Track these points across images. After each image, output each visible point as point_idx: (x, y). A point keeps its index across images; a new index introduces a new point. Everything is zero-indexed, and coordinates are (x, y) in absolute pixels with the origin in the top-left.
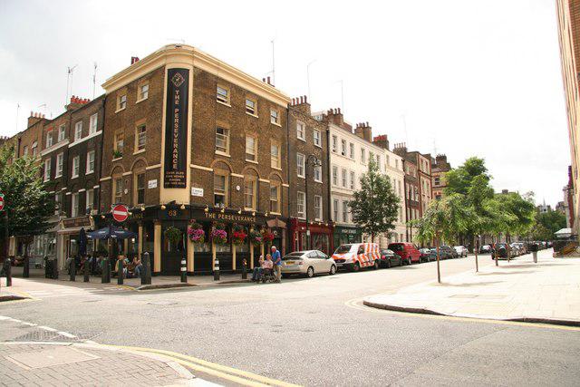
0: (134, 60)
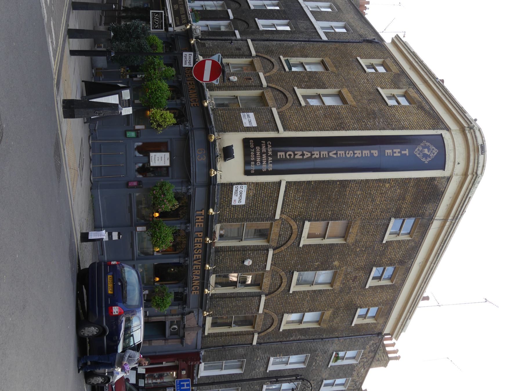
0: (443, 81)
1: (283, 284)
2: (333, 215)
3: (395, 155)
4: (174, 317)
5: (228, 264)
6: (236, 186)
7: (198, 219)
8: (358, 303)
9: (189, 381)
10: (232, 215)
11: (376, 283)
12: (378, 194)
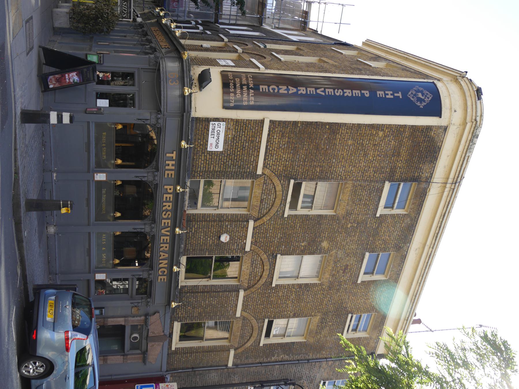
1: (264, 274)
2: (322, 172)
3: (387, 97)
4: (136, 319)
5: (202, 240)
6: (214, 123)
8: (348, 306)
10: (207, 166)
12: (371, 146)
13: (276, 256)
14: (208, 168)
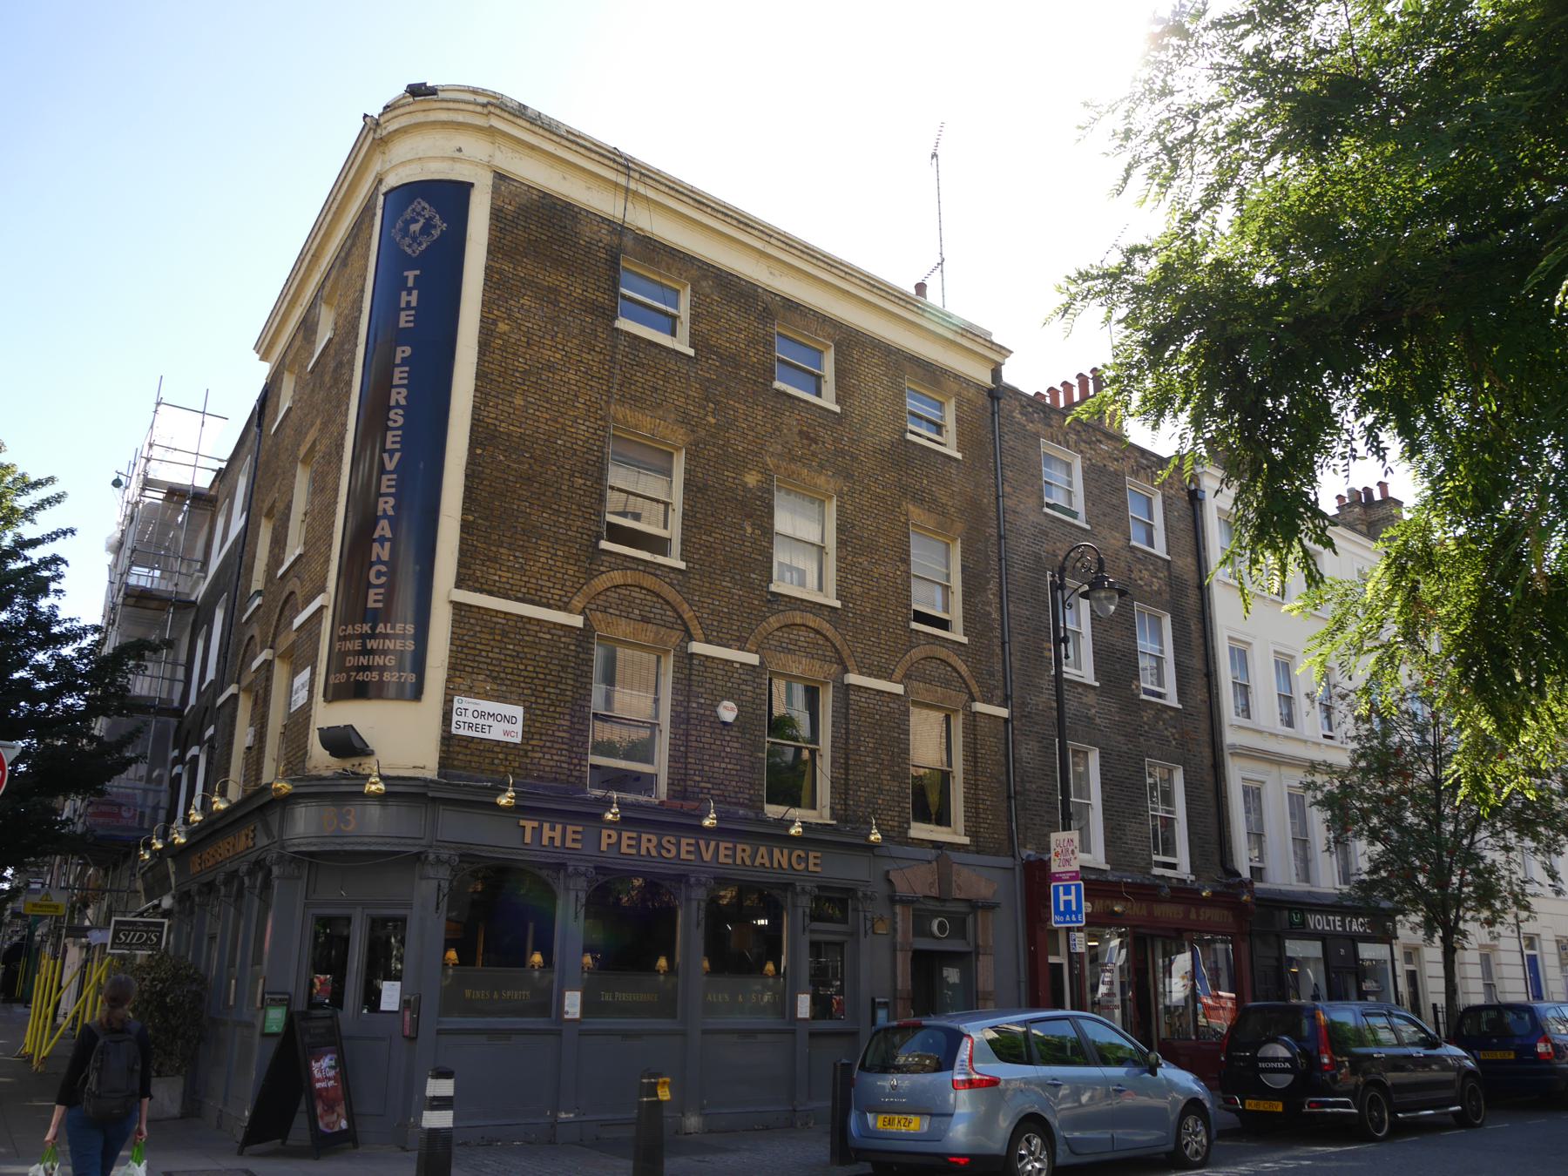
1: (811, 624)
3: (414, 304)
6: (454, 725)
7: (552, 839)
9: (1056, 888)
10: (556, 746)
11: (829, 388)
12: (531, 352)
13: (773, 594)
14: (563, 743)
